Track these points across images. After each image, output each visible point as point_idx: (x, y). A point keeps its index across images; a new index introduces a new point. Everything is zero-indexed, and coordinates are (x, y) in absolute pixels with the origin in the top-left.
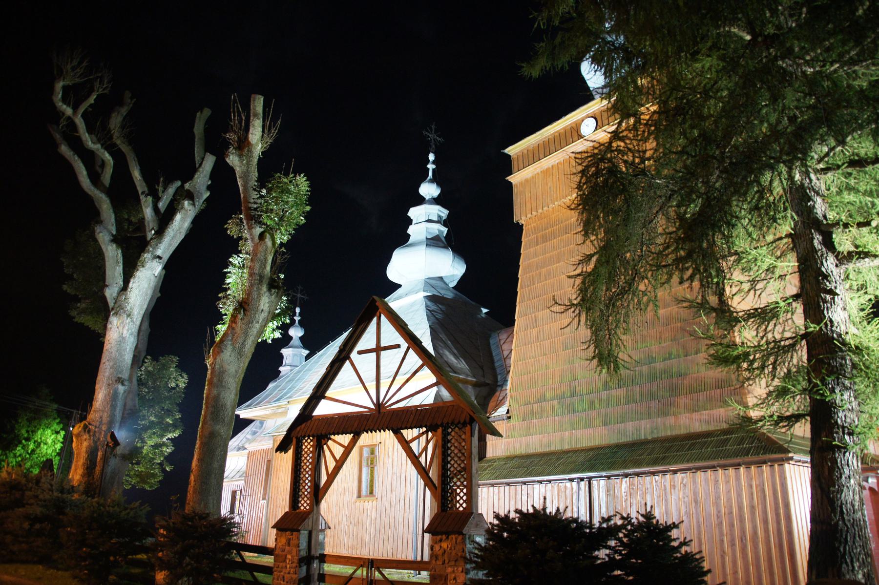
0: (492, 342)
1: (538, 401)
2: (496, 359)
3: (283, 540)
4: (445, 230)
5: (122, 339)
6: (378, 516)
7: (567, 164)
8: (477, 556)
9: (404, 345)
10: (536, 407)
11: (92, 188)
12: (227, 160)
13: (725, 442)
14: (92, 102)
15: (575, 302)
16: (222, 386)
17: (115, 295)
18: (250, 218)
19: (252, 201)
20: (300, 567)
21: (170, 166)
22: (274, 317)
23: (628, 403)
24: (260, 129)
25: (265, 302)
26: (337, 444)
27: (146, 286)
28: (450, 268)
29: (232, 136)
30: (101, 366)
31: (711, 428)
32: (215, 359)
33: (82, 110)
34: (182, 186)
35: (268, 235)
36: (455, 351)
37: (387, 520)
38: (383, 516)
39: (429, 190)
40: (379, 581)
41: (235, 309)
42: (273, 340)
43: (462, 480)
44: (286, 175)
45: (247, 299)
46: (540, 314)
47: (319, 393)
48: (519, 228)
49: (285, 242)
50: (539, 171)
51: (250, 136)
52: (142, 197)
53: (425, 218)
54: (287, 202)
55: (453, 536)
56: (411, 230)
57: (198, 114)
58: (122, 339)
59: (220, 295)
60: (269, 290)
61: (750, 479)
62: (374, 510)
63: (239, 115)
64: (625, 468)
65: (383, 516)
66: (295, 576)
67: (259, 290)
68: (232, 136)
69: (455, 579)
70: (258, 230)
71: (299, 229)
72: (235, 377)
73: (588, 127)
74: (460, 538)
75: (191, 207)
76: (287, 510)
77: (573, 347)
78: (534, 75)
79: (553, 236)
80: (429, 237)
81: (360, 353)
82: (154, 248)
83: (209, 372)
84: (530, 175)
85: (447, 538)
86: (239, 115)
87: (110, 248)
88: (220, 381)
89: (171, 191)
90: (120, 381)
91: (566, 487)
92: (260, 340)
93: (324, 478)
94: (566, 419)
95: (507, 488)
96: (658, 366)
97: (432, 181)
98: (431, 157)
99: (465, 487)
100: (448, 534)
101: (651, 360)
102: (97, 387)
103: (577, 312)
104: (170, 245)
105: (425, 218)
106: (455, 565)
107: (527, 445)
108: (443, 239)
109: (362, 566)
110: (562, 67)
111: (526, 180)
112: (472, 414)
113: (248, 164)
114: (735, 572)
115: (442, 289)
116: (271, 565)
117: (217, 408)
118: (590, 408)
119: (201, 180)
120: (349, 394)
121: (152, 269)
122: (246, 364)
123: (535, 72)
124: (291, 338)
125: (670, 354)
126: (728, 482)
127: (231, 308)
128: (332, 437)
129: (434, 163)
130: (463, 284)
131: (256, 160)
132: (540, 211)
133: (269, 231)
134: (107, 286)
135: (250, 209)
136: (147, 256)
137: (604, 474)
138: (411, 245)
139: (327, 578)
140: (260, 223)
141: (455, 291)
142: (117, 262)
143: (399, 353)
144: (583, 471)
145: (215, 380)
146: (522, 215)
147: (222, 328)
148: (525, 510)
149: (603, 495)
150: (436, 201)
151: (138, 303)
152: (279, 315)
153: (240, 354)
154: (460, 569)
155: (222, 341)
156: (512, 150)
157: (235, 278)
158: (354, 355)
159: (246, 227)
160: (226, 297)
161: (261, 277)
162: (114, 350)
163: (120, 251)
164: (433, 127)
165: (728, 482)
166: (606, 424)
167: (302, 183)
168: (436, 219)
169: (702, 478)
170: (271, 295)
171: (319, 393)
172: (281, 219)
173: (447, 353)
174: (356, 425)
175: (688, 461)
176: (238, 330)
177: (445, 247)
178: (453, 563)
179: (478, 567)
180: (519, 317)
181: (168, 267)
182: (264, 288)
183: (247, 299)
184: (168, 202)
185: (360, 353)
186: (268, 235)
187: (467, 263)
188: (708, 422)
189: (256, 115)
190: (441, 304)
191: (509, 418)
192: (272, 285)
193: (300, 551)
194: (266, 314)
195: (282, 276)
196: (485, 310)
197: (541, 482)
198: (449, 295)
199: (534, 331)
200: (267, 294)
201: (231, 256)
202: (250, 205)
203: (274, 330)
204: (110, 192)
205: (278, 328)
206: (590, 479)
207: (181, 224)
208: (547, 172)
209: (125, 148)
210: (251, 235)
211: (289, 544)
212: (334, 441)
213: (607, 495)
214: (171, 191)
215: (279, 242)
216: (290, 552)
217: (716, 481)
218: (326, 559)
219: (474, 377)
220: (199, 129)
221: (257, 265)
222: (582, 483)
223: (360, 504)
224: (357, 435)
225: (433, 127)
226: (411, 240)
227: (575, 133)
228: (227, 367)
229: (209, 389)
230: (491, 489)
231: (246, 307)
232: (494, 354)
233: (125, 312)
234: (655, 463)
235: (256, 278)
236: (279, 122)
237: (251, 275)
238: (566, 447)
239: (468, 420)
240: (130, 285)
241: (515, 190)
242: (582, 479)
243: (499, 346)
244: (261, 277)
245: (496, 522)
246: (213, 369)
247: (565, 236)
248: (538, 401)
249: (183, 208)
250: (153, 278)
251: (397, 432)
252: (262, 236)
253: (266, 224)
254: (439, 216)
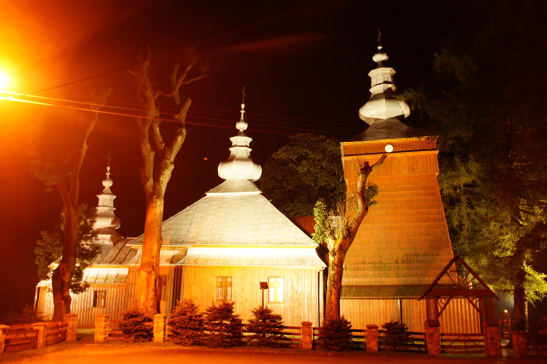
10: (361, 266)
17: (152, 184)
39: (242, 126)
93: (440, 310)
98: (243, 106)
101: (417, 255)
124: (104, 187)
125: (426, 254)
126: (457, 303)
150: (246, 133)
158: (448, 271)
165: (457, 303)
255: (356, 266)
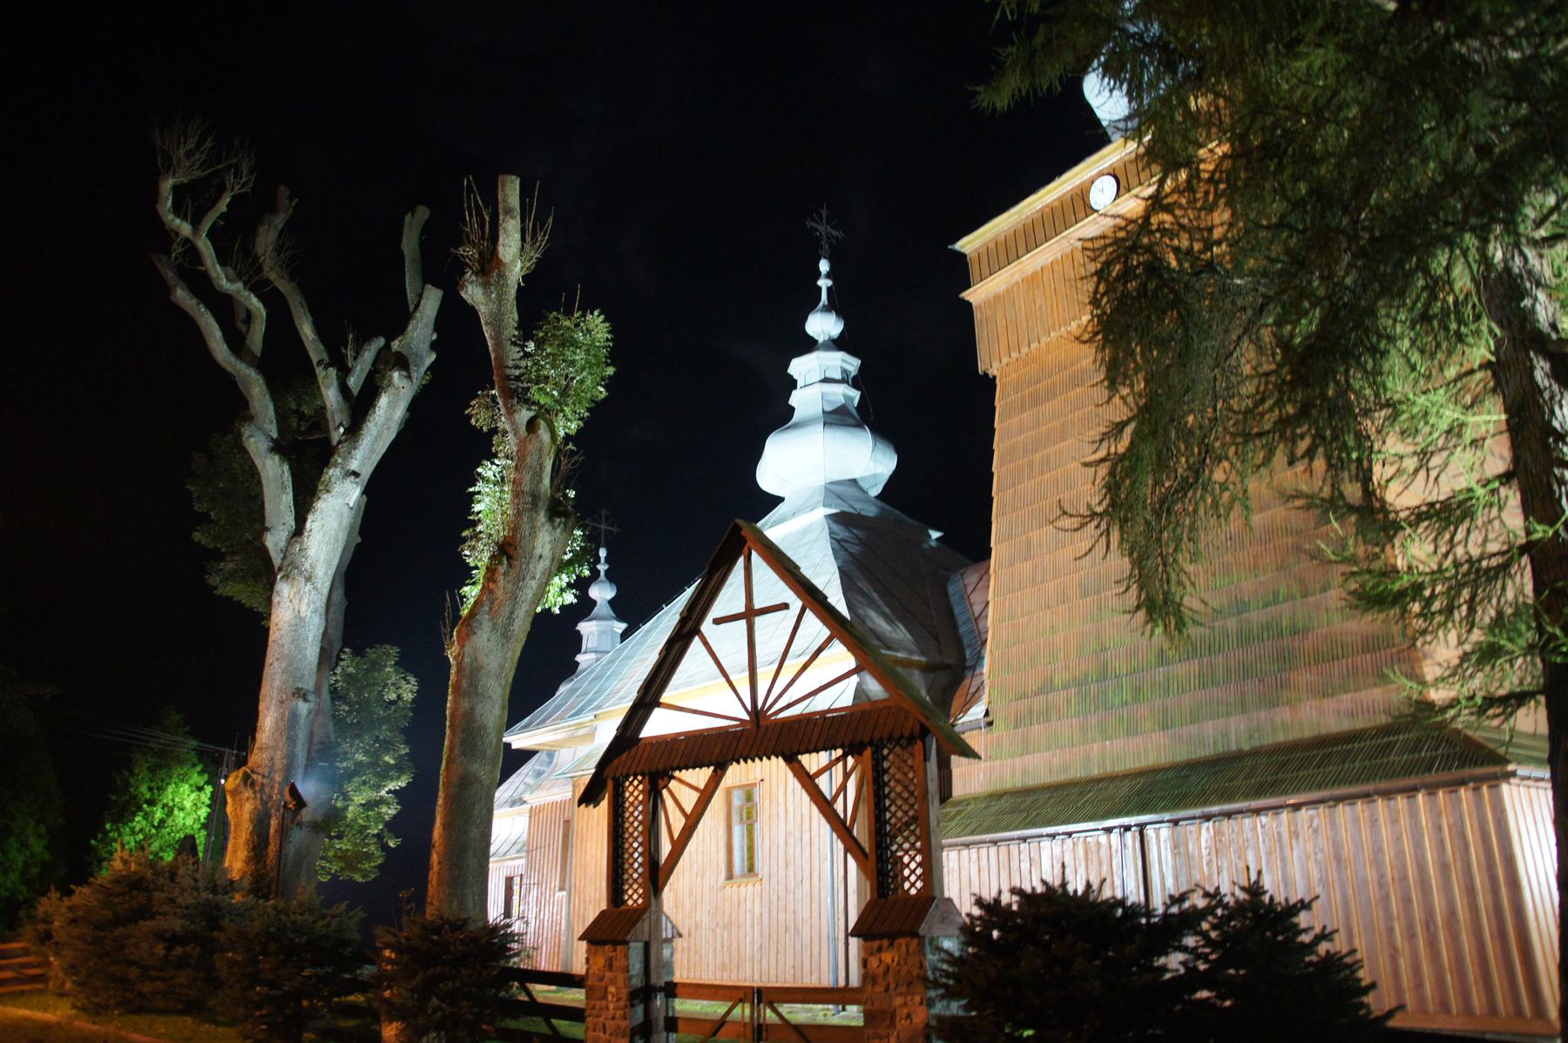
0: (951, 589)
1: (1040, 691)
2: (960, 620)
3: (600, 961)
4: (856, 395)
5: (299, 621)
6: (765, 910)
7: (1068, 264)
8: (948, 975)
9: (796, 604)
10: (1038, 703)
11: (233, 360)
12: (463, 294)
13: (1388, 748)
14: (224, 209)
15: (1099, 509)
16: (477, 694)
17: (283, 544)
18: (509, 394)
19: (511, 363)
20: (633, 1006)
21: (362, 308)
22: (562, 567)
23: (1203, 686)
24: (518, 236)
25: (545, 541)
26: (685, 786)
27: (335, 525)
28: (868, 461)
29: (469, 252)
30: (267, 671)
31: (1359, 724)
32: (462, 646)
33: (206, 225)
34: (387, 346)
35: (542, 423)
36: (887, 610)
37: (782, 917)
38: (774, 909)
39: (822, 325)
40: (774, 1026)
41: (492, 558)
42: (562, 608)
43: (912, 839)
44: (569, 313)
45: (513, 537)
46: (1035, 535)
47: (649, 697)
48: (989, 383)
49: (573, 433)
50: (1018, 277)
51: (500, 249)
52: (319, 371)
53: (819, 375)
54: (573, 363)
55: (903, 941)
56: (795, 399)
57: (408, 218)
58: (299, 621)
59: (465, 533)
60: (551, 519)
61: (1436, 814)
62: (757, 900)
63: (479, 214)
64: (1205, 803)
65: (774, 909)
66: (624, 1024)
67: (532, 520)
68: (469, 252)
69: (908, 1016)
70: (524, 415)
71: (597, 408)
72: (498, 677)
73: (1103, 194)
74: (915, 942)
75: (405, 383)
76: (604, 906)
77: (1098, 592)
78: (999, 105)
79: (1051, 394)
80: (829, 408)
81: (717, 621)
82: (344, 459)
83: (453, 671)
84: (1004, 287)
85: (891, 944)
86: (479, 214)
87: (269, 462)
88: (474, 684)
89: (368, 355)
90: (300, 694)
91: (1098, 844)
92: (539, 610)
93: (666, 848)
94: (1093, 721)
95: (993, 850)
96: (1256, 616)
97: (827, 309)
98: (824, 266)
99: (919, 851)
100: (892, 937)
101: (1241, 607)
102: (262, 706)
103: (1103, 526)
104: (372, 451)
105: (819, 375)
106: (907, 993)
107: (1025, 772)
108: (854, 412)
109: (741, 1000)
110: (1050, 88)
111: (997, 297)
112: (923, 720)
113: (500, 299)
114: (1419, 986)
115: (858, 500)
116: (582, 1006)
117: (470, 733)
118: (1136, 699)
119: (420, 334)
120: (702, 698)
121: (344, 495)
122: (518, 654)
123: (1002, 101)
124: (594, 602)
125: (1276, 595)
126: (1395, 821)
127: (486, 557)
128: (677, 774)
129: (828, 276)
130: (893, 490)
131: (513, 292)
132: (1025, 350)
133: (544, 414)
134: (268, 529)
135: (508, 378)
136: (333, 473)
137: (1167, 816)
138: (797, 426)
139: (680, 1025)
140: (528, 402)
141: (879, 503)
142: (284, 487)
143: (788, 618)
144: (1129, 813)
145: (465, 684)
146: (991, 361)
147: (471, 592)
148: (1028, 890)
149: (1167, 855)
150: (838, 344)
151: (322, 557)
152: (570, 562)
153: (506, 635)
154: (917, 999)
155: (472, 613)
156: (968, 244)
157: (490, 502)
158: (707, 627)
159: (503, 411)
160: (476, 536)
161: (535, 497)
162: (286, 640)
163: (286, 467)
164: (824, 212)
165: (1395, 821)
166: (1165, 726)
167: (597, 327)
168: (838, 376)
169: (1348, 817)
170: (554, 528)
171: (649, 697)
172: (564, 392)
173: (873, 614)
174: (717, 751)
175: (1319, 787)
176: (499, 593)
177: (858, 425)
178: (904, 989)
179: (950, 994)
180: (998, 542)
181: (377, 488)
182: (542, 517)
183: (513, 537)
184: (364, 375)
185: (717, 621)
186: (542, 423)
187: (898, 451)
188: (1352, 715)
189: (508, 212)
190: (857, 527)
191: (990, 724)
192: (556, 510)
193: (630, 978)
194: (547, 563)
195: (572, 494)
196: (935, 535)
197: (1053, 836)
198: (871, 511)
199: (1028, 565)
200: (547, 526)
201: (479, 464)
202: (508, 372)
203: (562, 590)
204: (262, 366)
205: (569, 585)
206: (1142, 827)
207: (389, 413)
208: (1032, 280)
209: (284, 286)
210: (513, 423)
211: (610, 967)
212: (681, 781)
213: (1175, 855)
214: (368, 355)
215: (562, 433)
216: (613, 982)
217: (1374, 822)
218: (678, 990)
219: (923, 653)
220: (410, 243)
221: (527, 477)
222: (1128, 834)
223: (732, 890)
224: (720, 769)
225: (824, 212)
226: (796, 417)
227: (1080, 204)
228: (483, 659)
229: (455, 702)
230: (965, 853)
231: (511, 552)
232: (956, 611)
233: (301, 573)
234: (1258, 792)
235: (526, 501)
236: (550, 220)
237: (517, 494)
238: (1096, 772)
239: (917, 731)
240: (308, 525)
241: (977, 316)
242: (1127, 828)
243: (964, 597)
244: (535, 497)
245: (976, 912)
246: (459, 665)
247: (1071, 394)
248: (1040, 691)
249: (390, 384)
250: (346, 511)
251: (791, 760)
252: (531, 425)
253: (538, 404)
254: (844, 371)
255: (1022, 705)
